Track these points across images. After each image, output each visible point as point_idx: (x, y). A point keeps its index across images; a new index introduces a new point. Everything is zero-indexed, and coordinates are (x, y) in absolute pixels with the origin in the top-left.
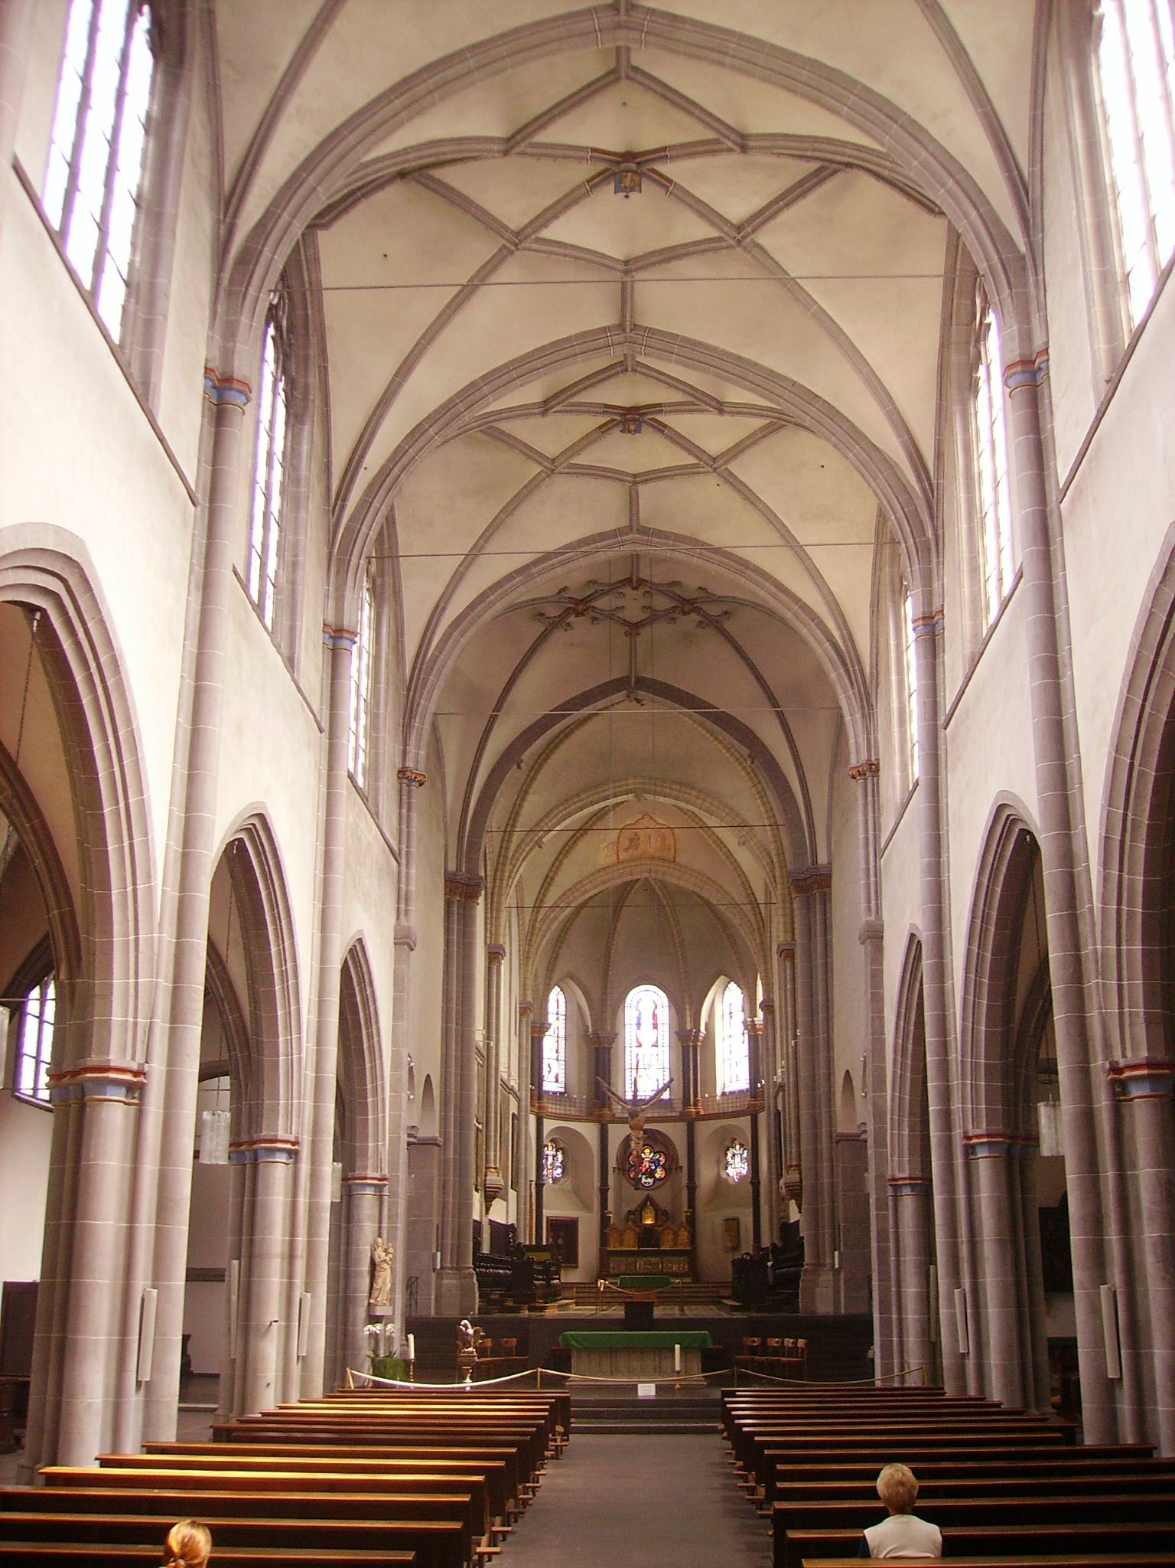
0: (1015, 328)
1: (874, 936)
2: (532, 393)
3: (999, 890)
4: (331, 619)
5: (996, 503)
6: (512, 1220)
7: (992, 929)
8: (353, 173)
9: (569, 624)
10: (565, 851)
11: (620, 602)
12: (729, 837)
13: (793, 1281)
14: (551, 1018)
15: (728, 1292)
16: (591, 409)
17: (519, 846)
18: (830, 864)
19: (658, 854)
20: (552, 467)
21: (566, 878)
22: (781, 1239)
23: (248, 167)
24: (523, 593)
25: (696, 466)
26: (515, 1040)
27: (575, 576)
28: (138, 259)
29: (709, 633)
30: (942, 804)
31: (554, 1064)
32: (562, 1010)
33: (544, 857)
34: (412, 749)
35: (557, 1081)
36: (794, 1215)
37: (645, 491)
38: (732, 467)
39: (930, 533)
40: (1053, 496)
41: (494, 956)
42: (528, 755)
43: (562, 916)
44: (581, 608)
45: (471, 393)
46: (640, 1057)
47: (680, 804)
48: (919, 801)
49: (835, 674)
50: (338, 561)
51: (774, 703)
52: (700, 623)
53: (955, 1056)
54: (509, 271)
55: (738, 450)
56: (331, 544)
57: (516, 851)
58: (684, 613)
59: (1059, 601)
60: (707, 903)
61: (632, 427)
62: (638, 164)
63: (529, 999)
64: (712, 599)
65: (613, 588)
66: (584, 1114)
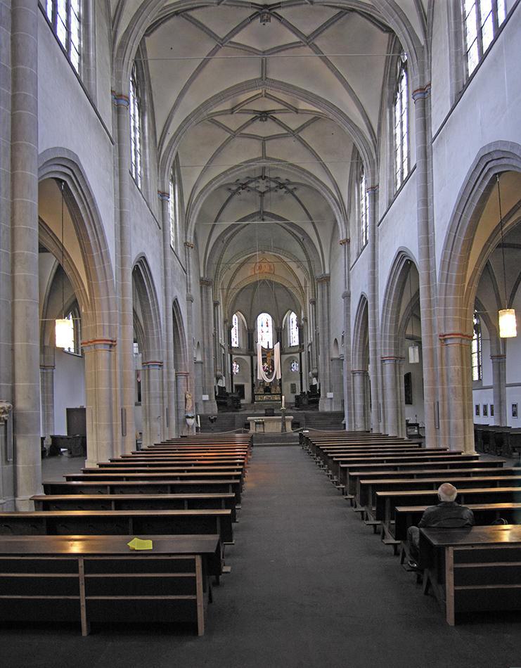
0: (418, 76)
1: (347, 296)
2: (227, 106)
3: (397, 280)
4: (160, 189)
5: (402, 145)
7: (394, 292)
8: (162, 10)
10: (238, 270)
11: (257, 185)
12: (293, 265)
13: (317, 402)
14: (234, 324)
15: (294, 405)
16: (248, 112)
18: (330, 274)
19: (268, 271)
20: (234, 135)
21: (238, 279)
22: (311, 389)
23: (120, 6)
24: (224, 181)
25: (287, 134)
27: (242, 175)
28: (82, 44)
30: (376, 252)
32: (237, 322)
33: (230, 273)
34: (188, 236)
36: (315, 382)
37: (268, 143)
38: (300, 134)
39: (375, 157)
40: (429, 141)
41: (216, 304)
43: (237, 292)
44: (244, 187)
45: (206, 105)
47: (276, 254)
48: (367, 250)
49: (335, 209)
50: (160, 168)
51: (311, 219)
52: (286, 192)
53: (378, 333)
54: (219, 54)
55: (302, 128)
56: (158, 162)
59: (429, 179)
60: (284, 287)
61: (264, 119)
62: (270, 10)
63: (227, 318)
65: (255, 179)
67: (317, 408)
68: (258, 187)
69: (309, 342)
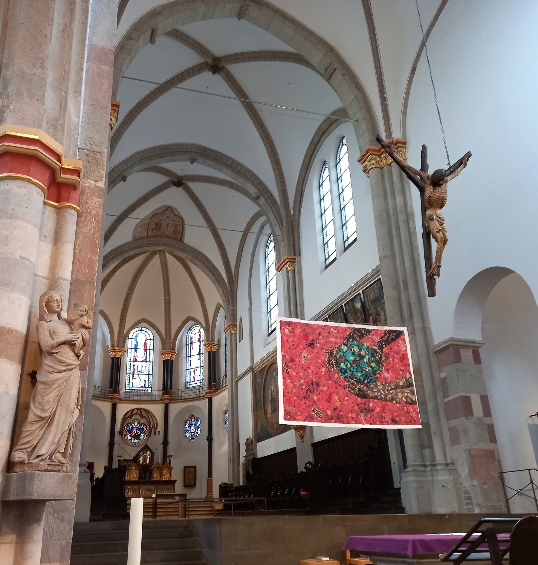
46: (136, 367)
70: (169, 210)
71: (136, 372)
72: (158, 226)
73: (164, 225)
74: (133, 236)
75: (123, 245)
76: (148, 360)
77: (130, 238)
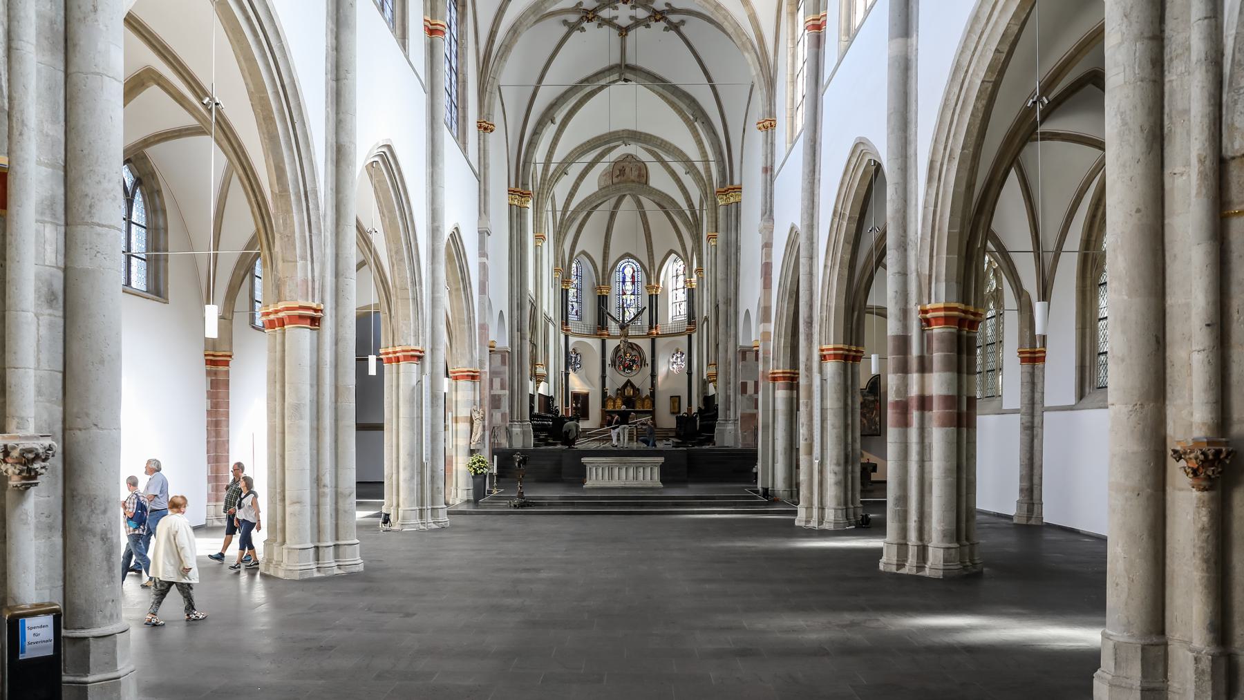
6: (552, 394)
9: (583, 28)
17: (553, 174)
19: (637, 180)
22: (704, 405)
26: (552, 290)
29: (672, 33)
31: (575, 304)
35: (577, 315)
36: (711, 390)
42: (559, 117)
44: (590, 16)
46: (625, 301)
52: (666, 27)
57: (551, 176)
58: (656, 21)
64: (674, 11)
66: (592, 333)
67: (710, 440)
68: (616, 18)
69: (705, 315)
70: (628, 157)
71: (625, 305)
72: (622, 172)
73: (627, 170)
74: (599, 186)
75: (590, 196)
76: (636, 293)
77: (597, 189)
